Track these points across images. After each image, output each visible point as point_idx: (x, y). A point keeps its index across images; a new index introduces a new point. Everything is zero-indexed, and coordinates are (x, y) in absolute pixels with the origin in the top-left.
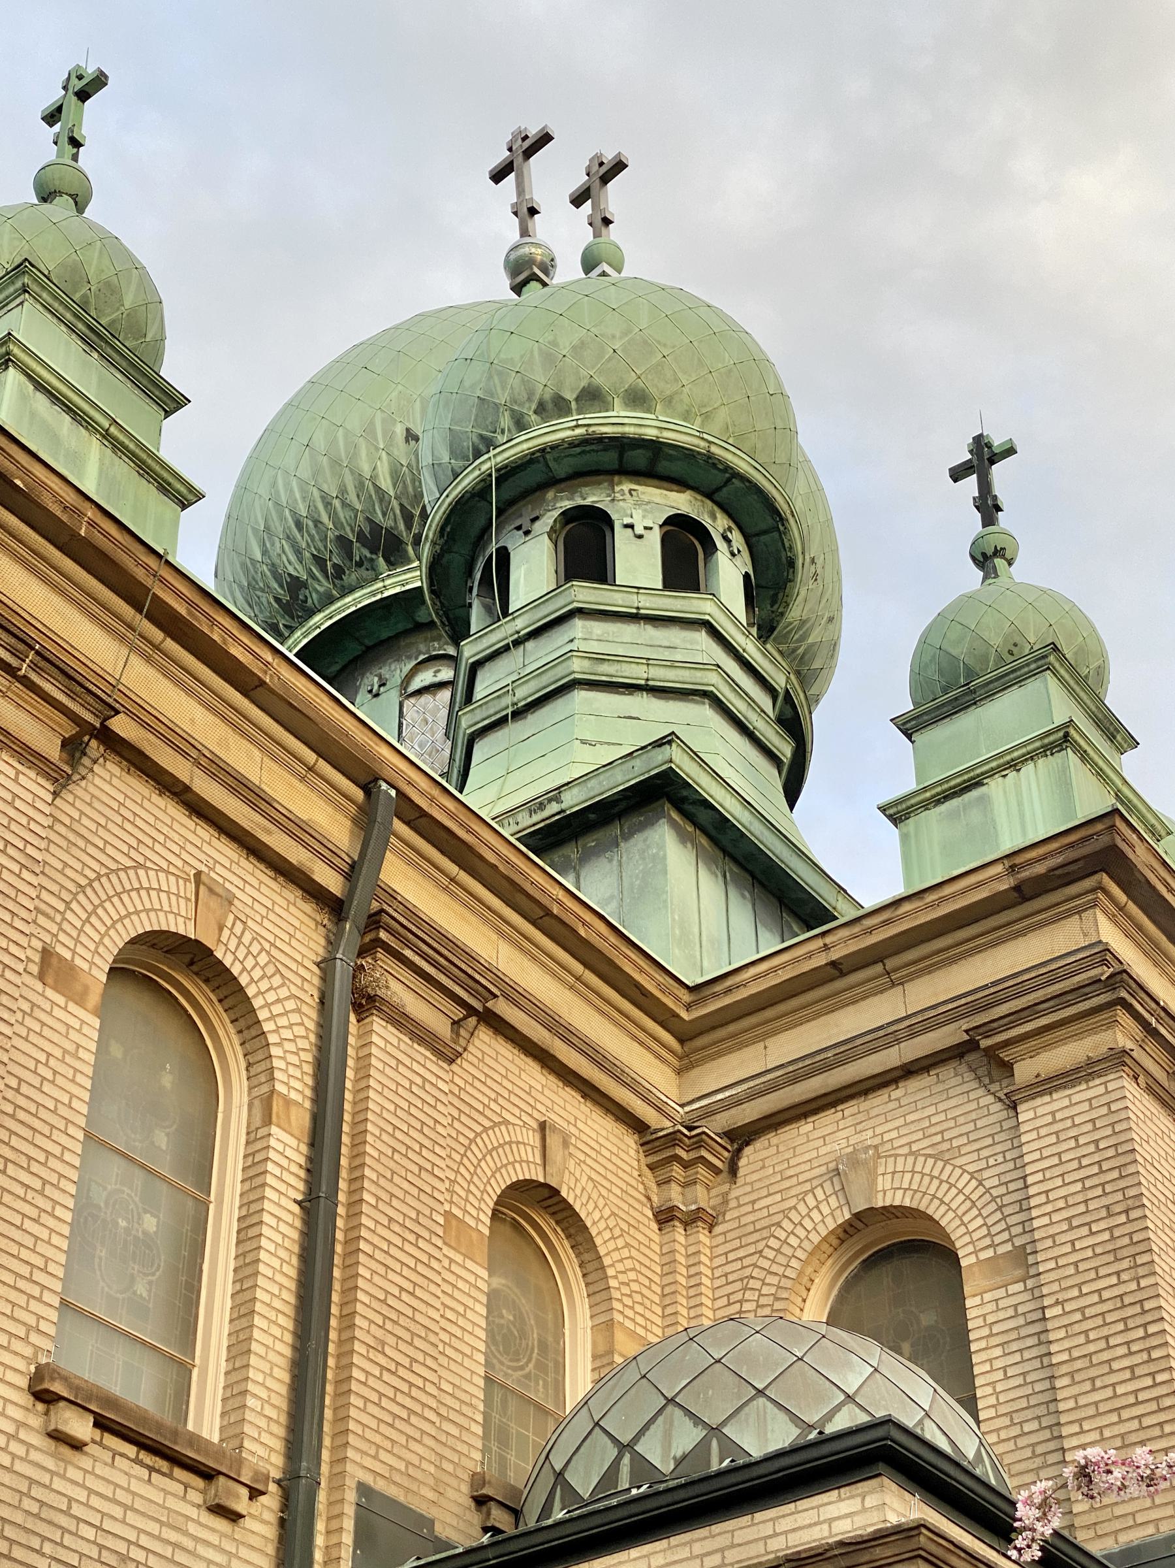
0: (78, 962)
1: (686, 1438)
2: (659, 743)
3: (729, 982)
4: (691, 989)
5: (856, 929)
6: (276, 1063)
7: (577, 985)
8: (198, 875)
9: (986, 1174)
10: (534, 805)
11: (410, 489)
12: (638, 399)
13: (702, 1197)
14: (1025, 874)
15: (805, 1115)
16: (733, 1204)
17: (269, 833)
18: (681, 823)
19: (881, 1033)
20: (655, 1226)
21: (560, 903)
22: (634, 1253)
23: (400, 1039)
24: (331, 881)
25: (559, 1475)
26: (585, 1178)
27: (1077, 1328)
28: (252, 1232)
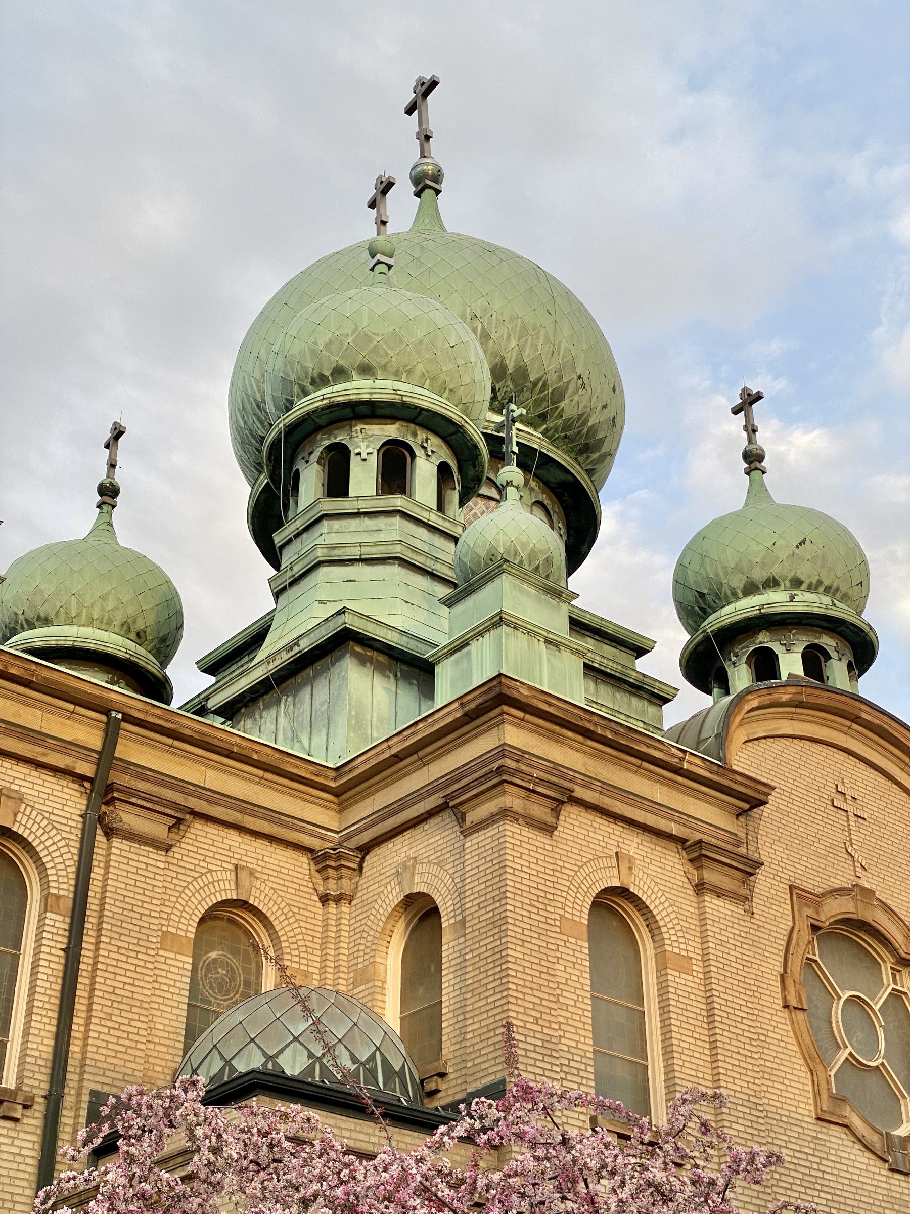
3: (350, 766)
5: (400, 737)
7: (261, 781)
10: (289, 647)
13: (346, 886)
14: (467, 708)
15: (391, 838)
16: (360, 888)
17: (44, 755)
18: (362, 652)
19: (416, 794)
20: (319, 905)
22: (302, 924)
23: (131, 846)
24: (86, 769)
26: (268, 888)
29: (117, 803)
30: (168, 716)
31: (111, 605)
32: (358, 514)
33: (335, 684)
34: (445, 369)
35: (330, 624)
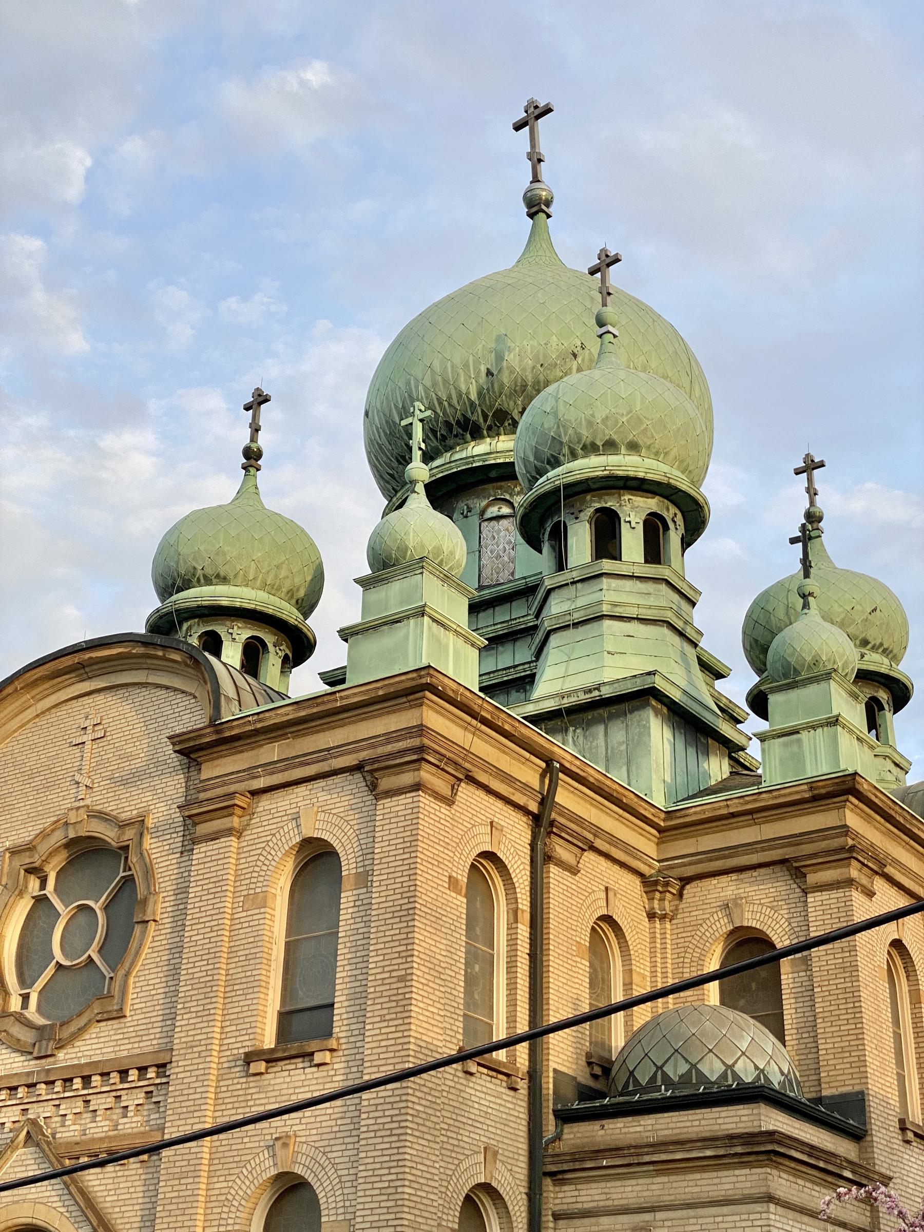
0: (460, 877)
1: (683, 1068)
2: (649, 674)
3: (683, 812)
6: (519, 895)
8: (492, 823)
9: (792, 920)
11: (488, 402)
21: (616, 791)
24: (534, 807)
25: (632, 1073)
27: (826, 999)
28: (513, 970)
29: (552, 836)
30: (583, 767)
31: (283, 573)
32: (632, 577)
33: (635, 730)
34: (691, 454)
35: (638, 680)
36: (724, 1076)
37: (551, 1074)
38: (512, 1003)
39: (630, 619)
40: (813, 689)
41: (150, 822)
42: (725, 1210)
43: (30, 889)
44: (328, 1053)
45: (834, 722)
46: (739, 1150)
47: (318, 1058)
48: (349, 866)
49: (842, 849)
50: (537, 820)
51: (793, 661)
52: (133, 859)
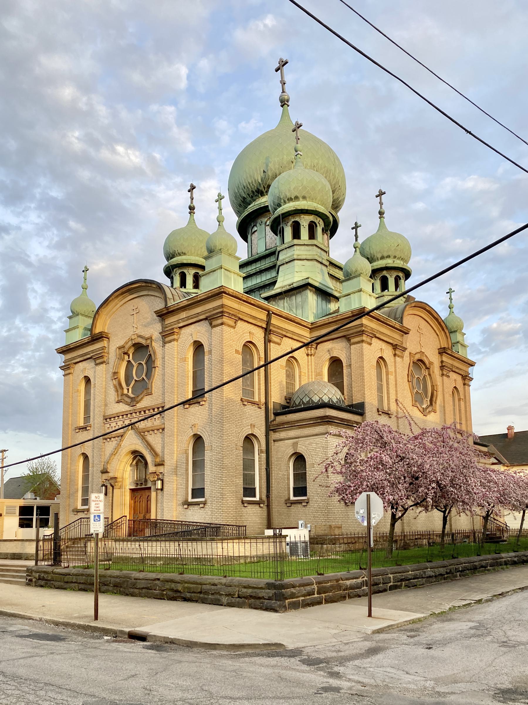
1: (308, 399)
2: (307, 278)
4: (312, 323)
12: (304, 198)
24: (264, 326)
25: (294, 401)
32: (304, 245)
36: (319, 401)
37: (272, 403)
38: (259, 384)
39: (303, 260)
40: (355, 280)
41: (154, 338)
42: (316, 437)
43: (125, 359)
44: (204, 402)
45: (360, 291)
46: (319, 421)
47: (201, 403)
48: (206, 349)
49: (360, 331)
50: (266, 329)
51: (349, 271)
52: (150, 349)
